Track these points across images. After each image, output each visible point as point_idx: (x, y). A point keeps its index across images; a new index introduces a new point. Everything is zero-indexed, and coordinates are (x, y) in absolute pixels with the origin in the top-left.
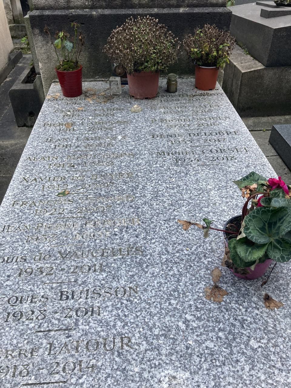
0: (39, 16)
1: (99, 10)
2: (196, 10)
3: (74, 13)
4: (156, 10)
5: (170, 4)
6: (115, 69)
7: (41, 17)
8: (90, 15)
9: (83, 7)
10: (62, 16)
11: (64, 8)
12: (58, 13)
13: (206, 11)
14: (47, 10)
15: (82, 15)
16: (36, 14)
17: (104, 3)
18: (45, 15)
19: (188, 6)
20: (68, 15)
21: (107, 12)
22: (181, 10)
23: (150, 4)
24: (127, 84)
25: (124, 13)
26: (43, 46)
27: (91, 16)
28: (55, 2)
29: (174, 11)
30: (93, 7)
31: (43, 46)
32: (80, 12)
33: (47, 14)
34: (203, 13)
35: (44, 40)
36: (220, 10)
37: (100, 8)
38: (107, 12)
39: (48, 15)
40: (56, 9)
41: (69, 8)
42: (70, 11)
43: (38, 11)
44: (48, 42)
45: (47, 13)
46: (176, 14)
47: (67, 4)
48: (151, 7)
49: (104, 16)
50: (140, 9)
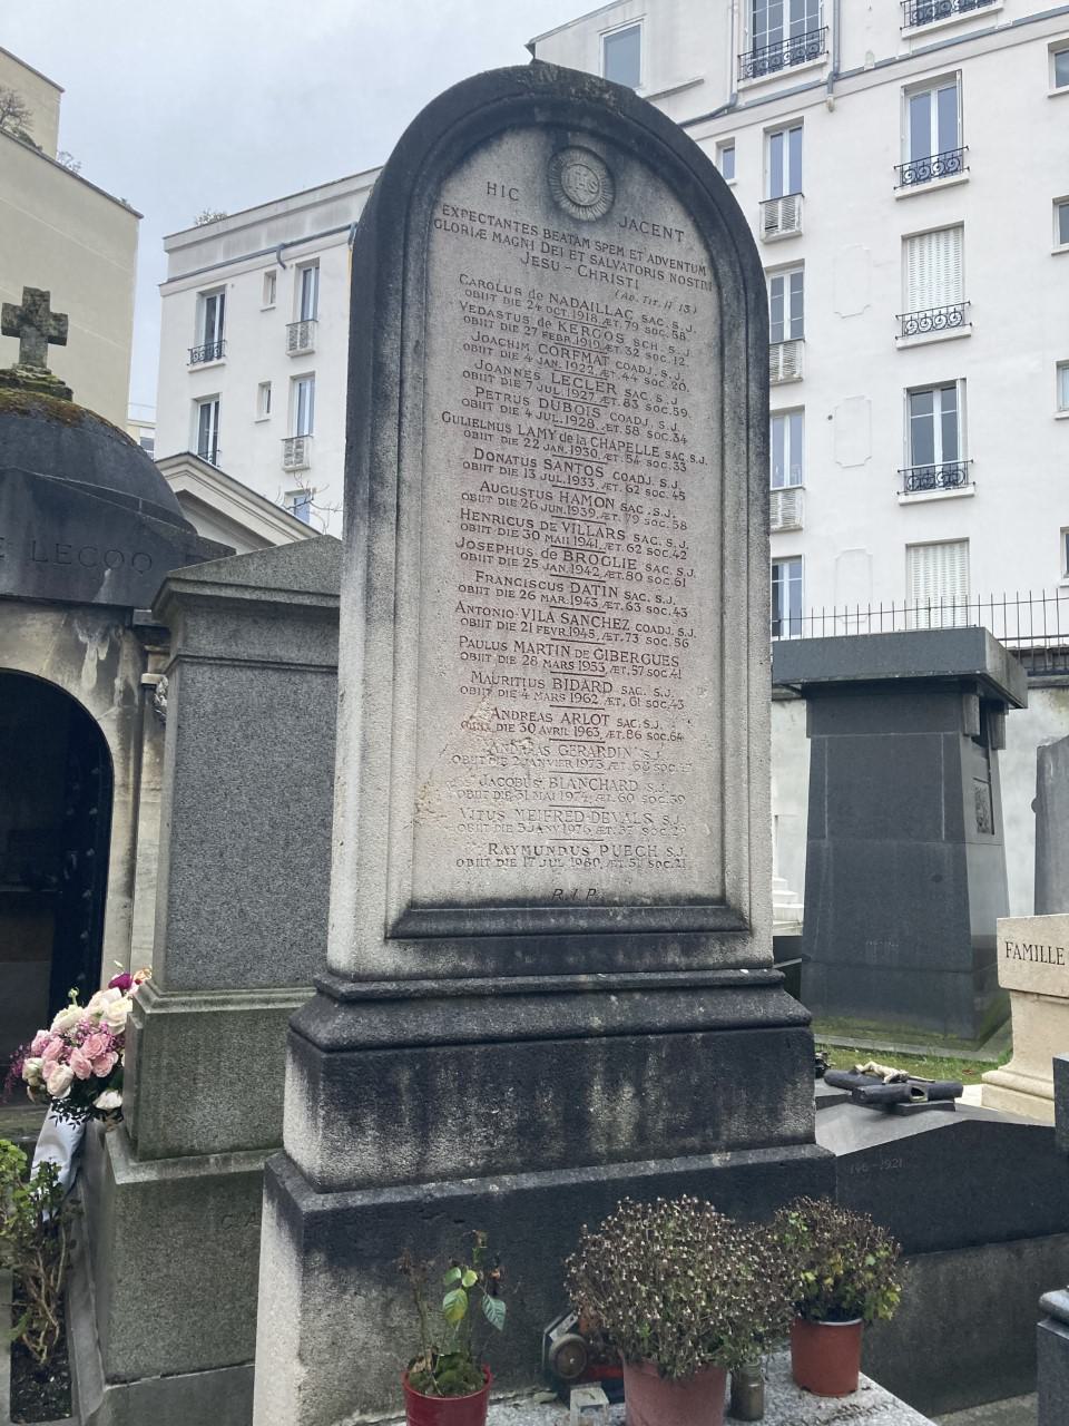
0: (334, 1213)
1: (506, 1178)
2: (752, 1158)
3: (438, 1195)
4: (652, 1164)
5: (684, 1147)
6: (557, 1356)
7: (339, 1217)
8: (485, 1194)
9: (458, 1175)
10: (402, 1206)
11: (406, 1181)
12: (389, 1196)
13: (777, 1158)
14: (355, 1189)
15: (461, 1198)
16: (328, 1206)
17: (518, 1159)
18: (356, 1208)
19: (729, 1148)
20: (420, 1201)
21: (529, 1181)
22: (716, 1160)
23: (636, 1150)
24: (623, 1401)
25: (574, 1180)
26: (327, 1304)
27: (488, 1196)
28: (384, 1167)
29: (697, 1164)
30: (487, 1172)
31: (327, 1304)
32: (453, 1189)
33: (359, 1203)
34: (769, 1164)
35: (334, 1284)
36: (520, 98)
37: (505, 1173)
38: (529, 1181)
39: (363, 1207)
40: (382, 1186)
41: (420, 1179)
42: (425, 1187)
43: (330, 1196)
44: (344, 1290)
45: (359, 1199)
46: (701, 1172)
47: (418, 1170)
48: (638, 1158)
49: (521, 1195)
50: (612, 1166)
